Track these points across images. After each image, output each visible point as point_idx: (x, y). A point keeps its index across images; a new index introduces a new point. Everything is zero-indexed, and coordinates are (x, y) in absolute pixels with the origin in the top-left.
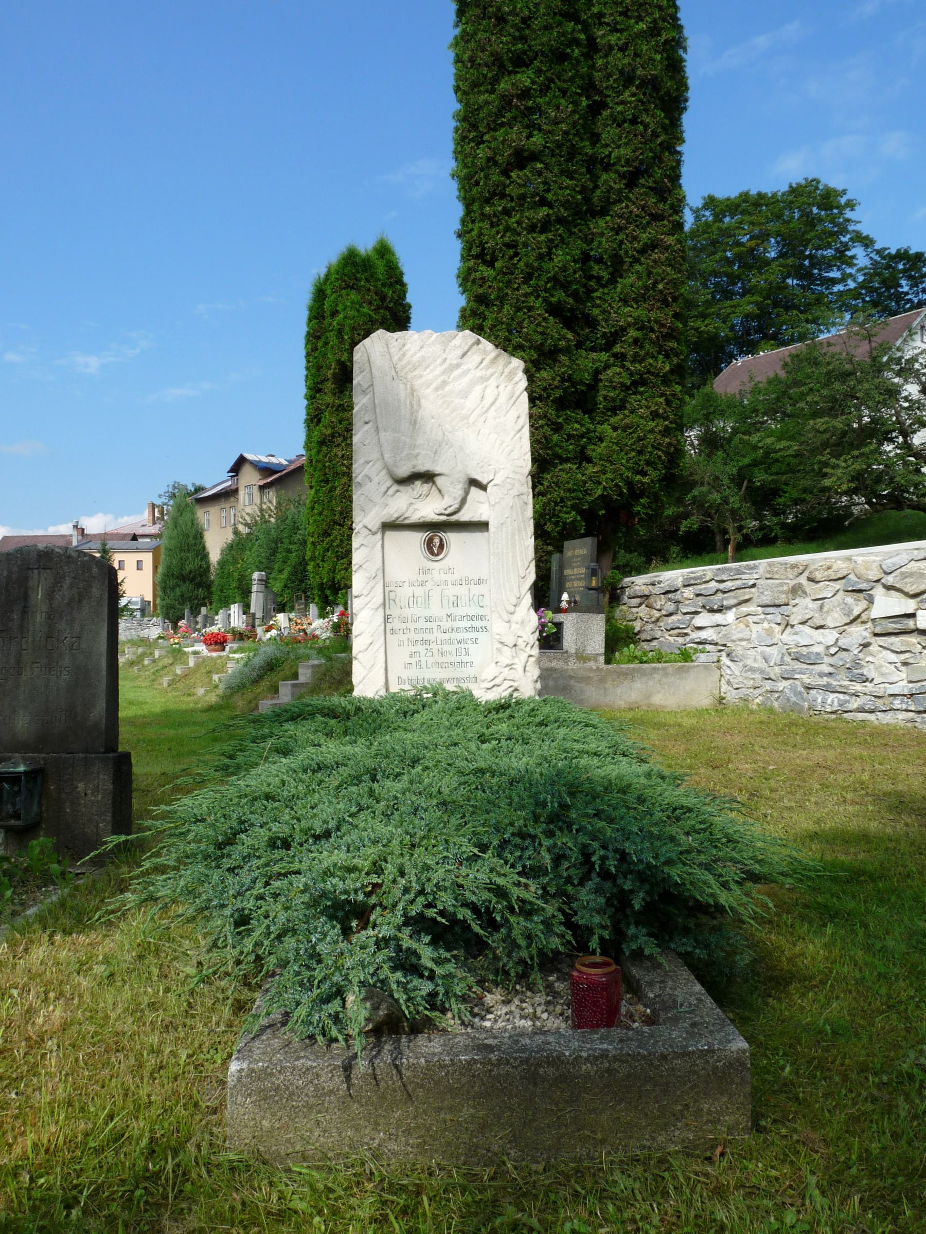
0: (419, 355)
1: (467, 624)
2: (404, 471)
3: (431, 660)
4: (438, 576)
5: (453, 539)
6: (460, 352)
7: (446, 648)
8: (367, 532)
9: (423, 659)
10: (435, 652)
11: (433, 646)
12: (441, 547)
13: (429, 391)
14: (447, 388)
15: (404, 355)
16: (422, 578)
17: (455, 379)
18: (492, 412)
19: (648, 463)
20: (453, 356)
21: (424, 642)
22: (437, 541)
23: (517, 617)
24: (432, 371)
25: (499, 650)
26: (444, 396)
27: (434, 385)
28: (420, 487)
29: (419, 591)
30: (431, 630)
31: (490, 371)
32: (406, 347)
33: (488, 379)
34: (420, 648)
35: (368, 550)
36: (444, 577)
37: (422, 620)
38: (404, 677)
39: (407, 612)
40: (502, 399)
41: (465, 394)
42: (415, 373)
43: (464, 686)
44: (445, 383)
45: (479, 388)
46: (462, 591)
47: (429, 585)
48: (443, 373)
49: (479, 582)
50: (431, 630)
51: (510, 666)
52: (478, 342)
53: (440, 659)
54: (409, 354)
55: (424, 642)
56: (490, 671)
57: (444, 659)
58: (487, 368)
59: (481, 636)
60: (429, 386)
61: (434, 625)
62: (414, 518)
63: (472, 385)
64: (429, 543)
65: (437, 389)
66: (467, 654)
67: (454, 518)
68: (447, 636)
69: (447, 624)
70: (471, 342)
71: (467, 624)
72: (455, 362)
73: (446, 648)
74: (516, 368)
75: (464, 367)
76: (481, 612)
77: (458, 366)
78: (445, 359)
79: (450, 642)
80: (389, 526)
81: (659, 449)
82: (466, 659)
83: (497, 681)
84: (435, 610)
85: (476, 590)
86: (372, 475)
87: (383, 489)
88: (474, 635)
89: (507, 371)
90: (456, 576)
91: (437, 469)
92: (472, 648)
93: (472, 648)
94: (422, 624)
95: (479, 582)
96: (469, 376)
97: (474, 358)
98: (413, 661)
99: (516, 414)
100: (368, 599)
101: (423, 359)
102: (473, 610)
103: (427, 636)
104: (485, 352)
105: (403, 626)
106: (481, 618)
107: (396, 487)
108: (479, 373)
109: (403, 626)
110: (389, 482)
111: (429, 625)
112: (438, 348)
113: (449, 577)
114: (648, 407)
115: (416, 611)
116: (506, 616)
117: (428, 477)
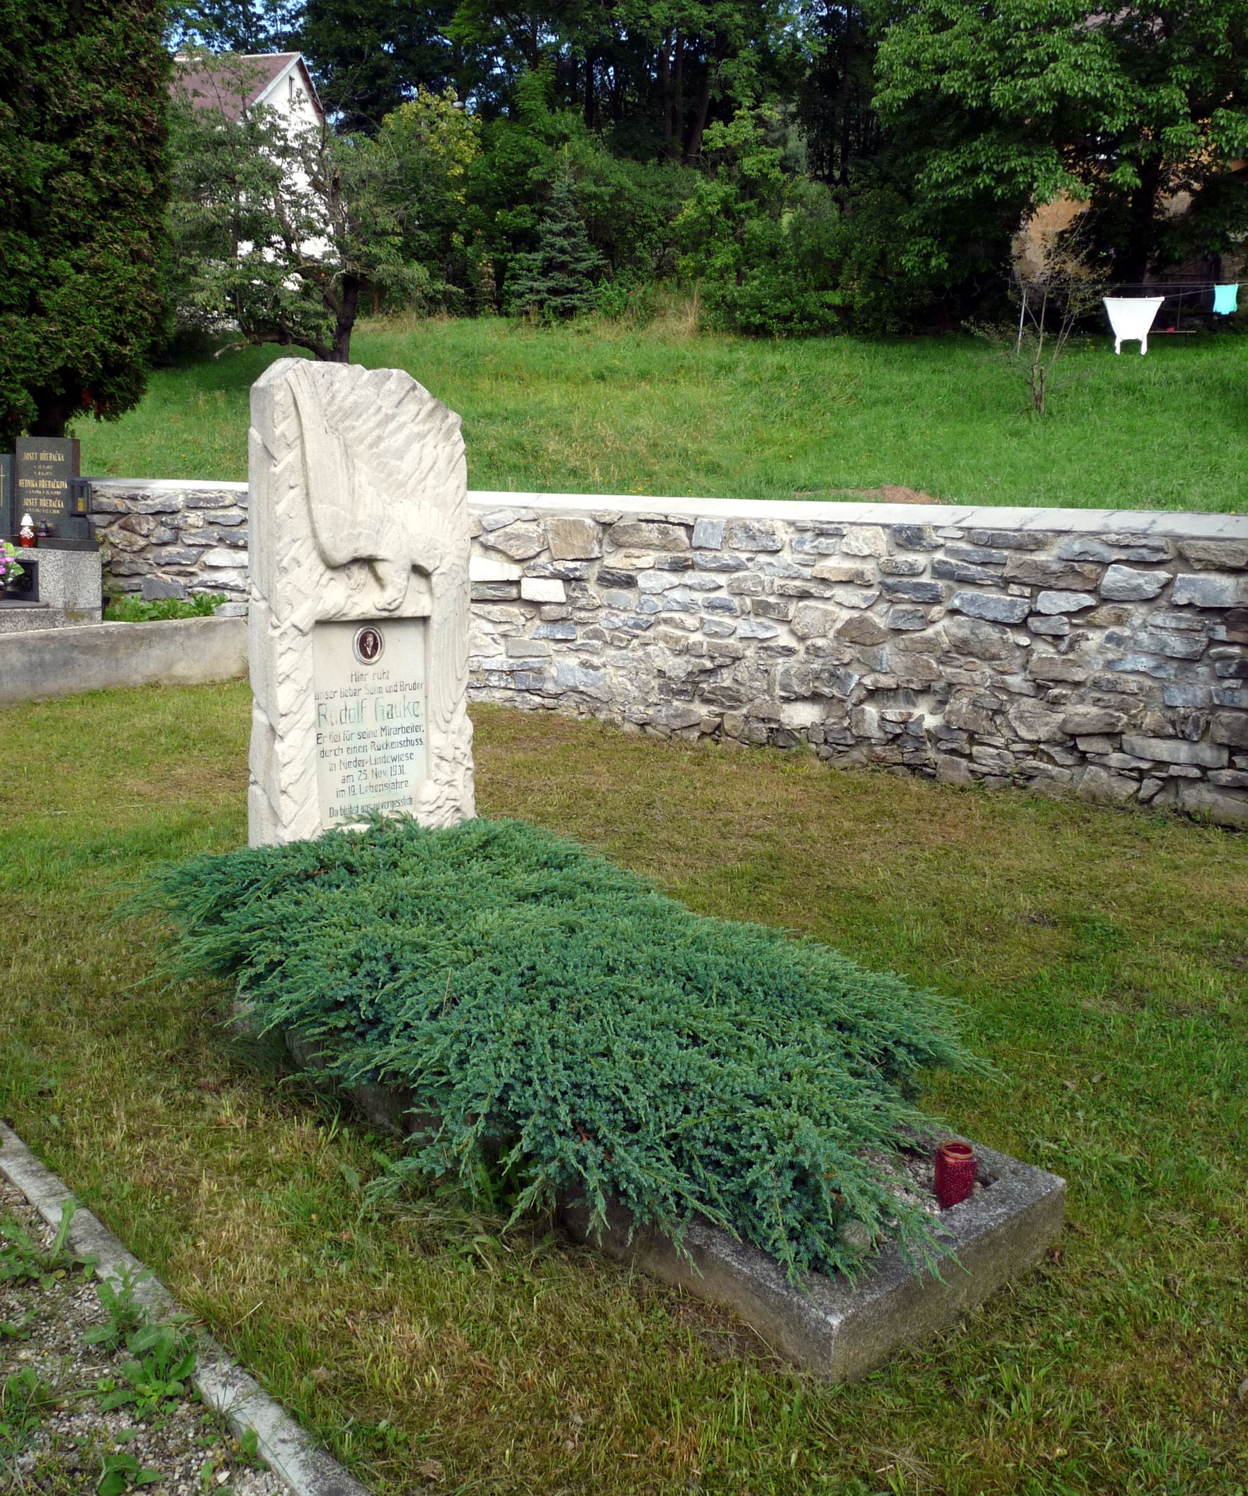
0: (351, 399)
1: (401, 737)
2: (342, 556)
3: (365, 784)
4: (371, 682)
5: (390, 636)
6: (395, 399)
7: (380, 767)
8: (296, 632)
9: (356, 783)
10: (369, 773)
11: (367, 766)
12: (375, 647)
13: (362, 447)
14: (382, 446)
15: (333, 397)
16: (354, 685)
17: (392, 434)
18: (431, 480)
19: (130, 326)
20: (387, 405)
21: (358, 763)
22: (370, 639)
23: (454, 726)
24: (365, 422)
25: (437, 766)
26: (379, 456)
27: (369, 440)
28: (360, 574)
29: (352, 702)
30: (364, 749)
31: (428, 426)
32: (336, 386)
33: (425, 436)
34: (354, 771)
35: (296, 655)
36: (378, 683)
37: (355, 737)
38: (337, 807)
39: (339, 729)
40: (441, 464)
41: (400, 454)
42: (347, 423)
43: (403, 809)
44: (380, 439)
45: (416, 446)
46: (396, 698)
47: (362, 694)
48: (378, 425)
49: (415, 687)
50: (364, 749)
51: (450, 783)
52: (414, 388)
53: (375, 782)
54: (340, 397)
55: (358, 763)
56: (429, 791)
57: (379, 781)
58: (425, 421)
59: (417, 750)
60: (361, 441)
61: (367, 742)
62: (354, 614)
63: (409, 442)
64: (363, 642)
65: (371, 446)
66: (402, 772)
67: (397, 614)
68: (380, 754)
69: (381, 740)
70: (407, 387)
71: (401, 737)
72: (390, 412)
73: (380, 767)
74: (453, 425)
75: (401, 419)
76: (416, 722)
77: (393, 417)
78: (380, 408)
79: (384, 760)
80: (323, 623)
81: (145, 309)
82: (400, 778)
83: (439, 803)
84: (370, 724)
85: (413, 696)
86: (301, 558)
87: (316, 577)
88: (409, 749)
89: (445, 427)
90: (391, 682)
91: (381, 554)
92: (408, 765)
93: (408, 765)
94: (355, 742)
95: (415, 687)
96: (406, 432)
97: (411, 408)
98: (345, 787)
99: (456, 483)
100: (298, 717)
101: (356, 405)
102: (408, 721)
103: (360, 756)
104: (422, 402)
105: (335, 746)
106: (416, 729)
107: (329, 574)
108: (416, 429)
109: (335, 746)
110: (322, 568)
111: (362, 742)
112: (371, 391)
113: (384, 684)
114: (126, 243)
115: (348, 727)
116: (443, 725)
117: (368, 562)
